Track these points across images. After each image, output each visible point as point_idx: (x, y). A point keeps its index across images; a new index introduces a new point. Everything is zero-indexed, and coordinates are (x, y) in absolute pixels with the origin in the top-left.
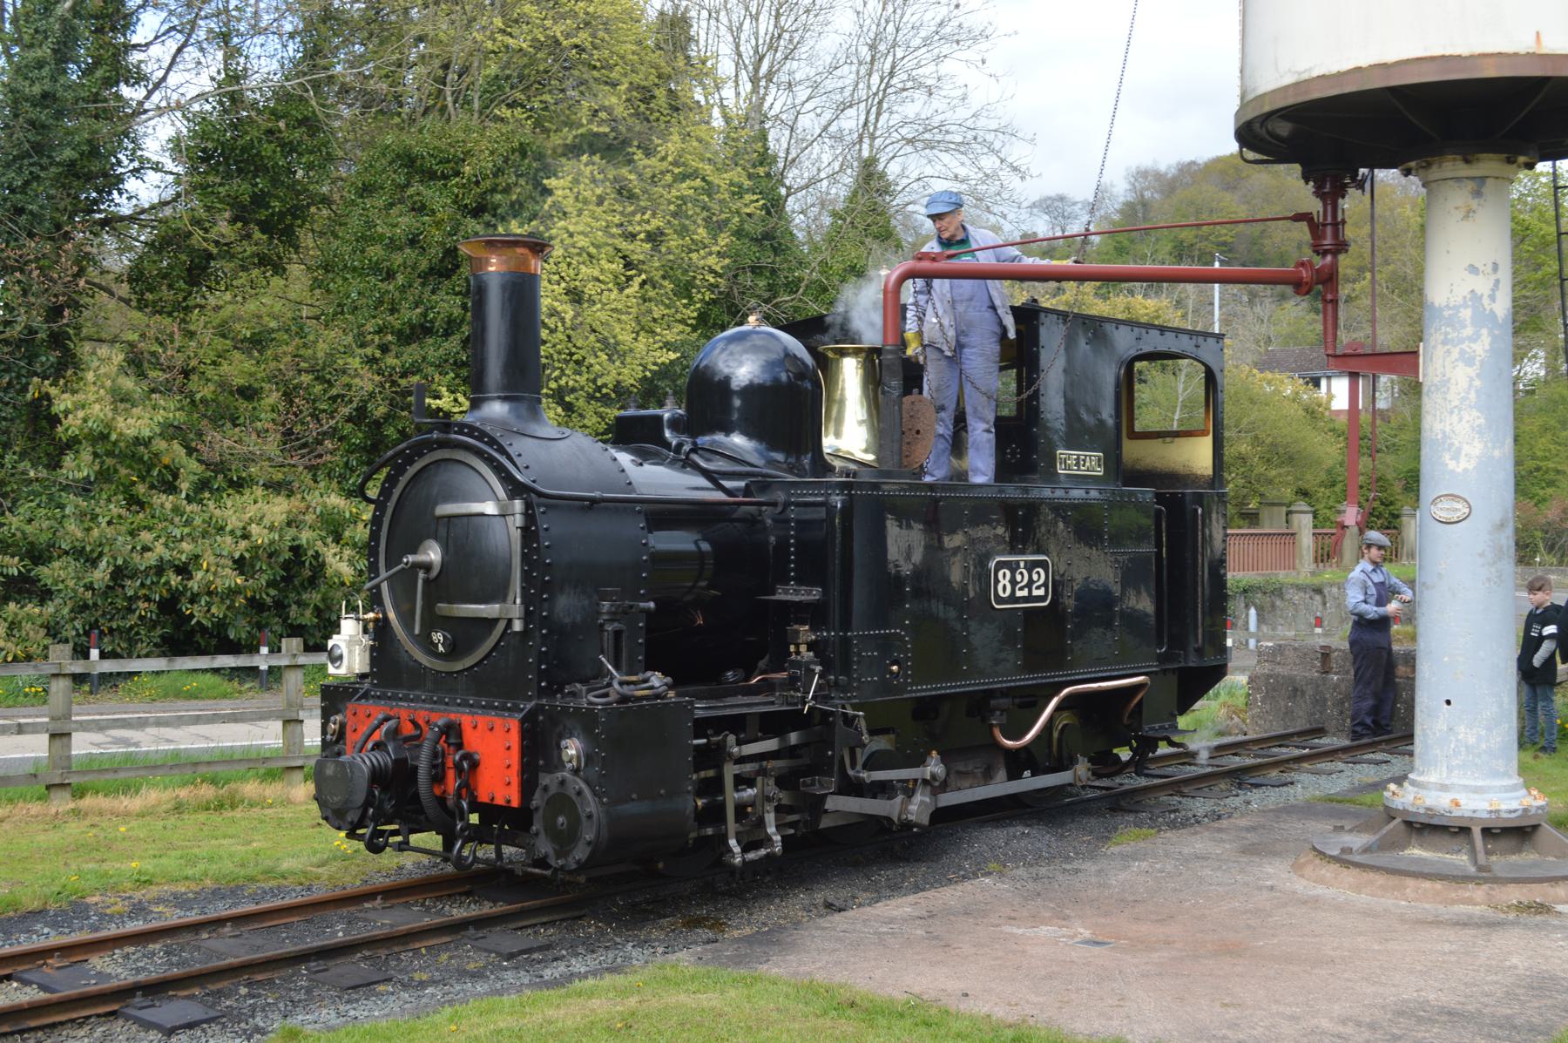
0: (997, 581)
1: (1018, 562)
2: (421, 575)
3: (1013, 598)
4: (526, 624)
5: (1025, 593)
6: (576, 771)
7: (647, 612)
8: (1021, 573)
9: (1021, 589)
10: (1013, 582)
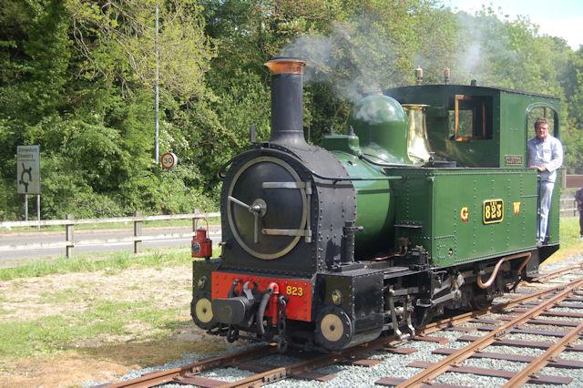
3: (491, 219)
4: (312, 239)
5: (494, 216)
10: (491, 211)
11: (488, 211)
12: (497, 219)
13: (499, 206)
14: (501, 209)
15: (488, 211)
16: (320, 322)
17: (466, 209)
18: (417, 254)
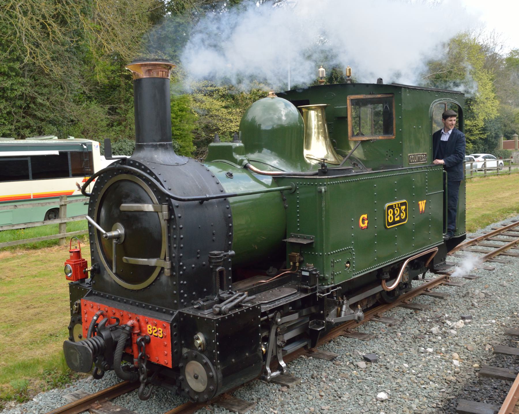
0: (388, 215)
1: (395, 205)
2: (114, 241)
3: (394, 222)
6: (202, 352)
7: (232, 256)
8: (397, 210)
9: (397, 217)
10: (394, 214)
11: (391, 215)
12: (401, 220)
13: (403, 207)
14: (405, 210)
15: (391, 215)
16: (183, 368)
17: (365, 216)
18: (307, 274)
